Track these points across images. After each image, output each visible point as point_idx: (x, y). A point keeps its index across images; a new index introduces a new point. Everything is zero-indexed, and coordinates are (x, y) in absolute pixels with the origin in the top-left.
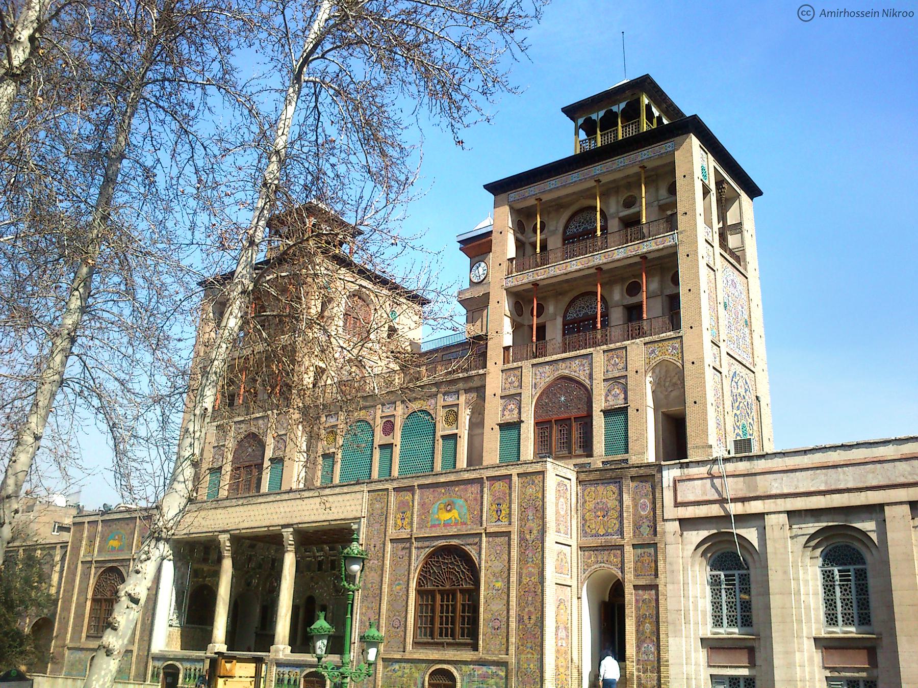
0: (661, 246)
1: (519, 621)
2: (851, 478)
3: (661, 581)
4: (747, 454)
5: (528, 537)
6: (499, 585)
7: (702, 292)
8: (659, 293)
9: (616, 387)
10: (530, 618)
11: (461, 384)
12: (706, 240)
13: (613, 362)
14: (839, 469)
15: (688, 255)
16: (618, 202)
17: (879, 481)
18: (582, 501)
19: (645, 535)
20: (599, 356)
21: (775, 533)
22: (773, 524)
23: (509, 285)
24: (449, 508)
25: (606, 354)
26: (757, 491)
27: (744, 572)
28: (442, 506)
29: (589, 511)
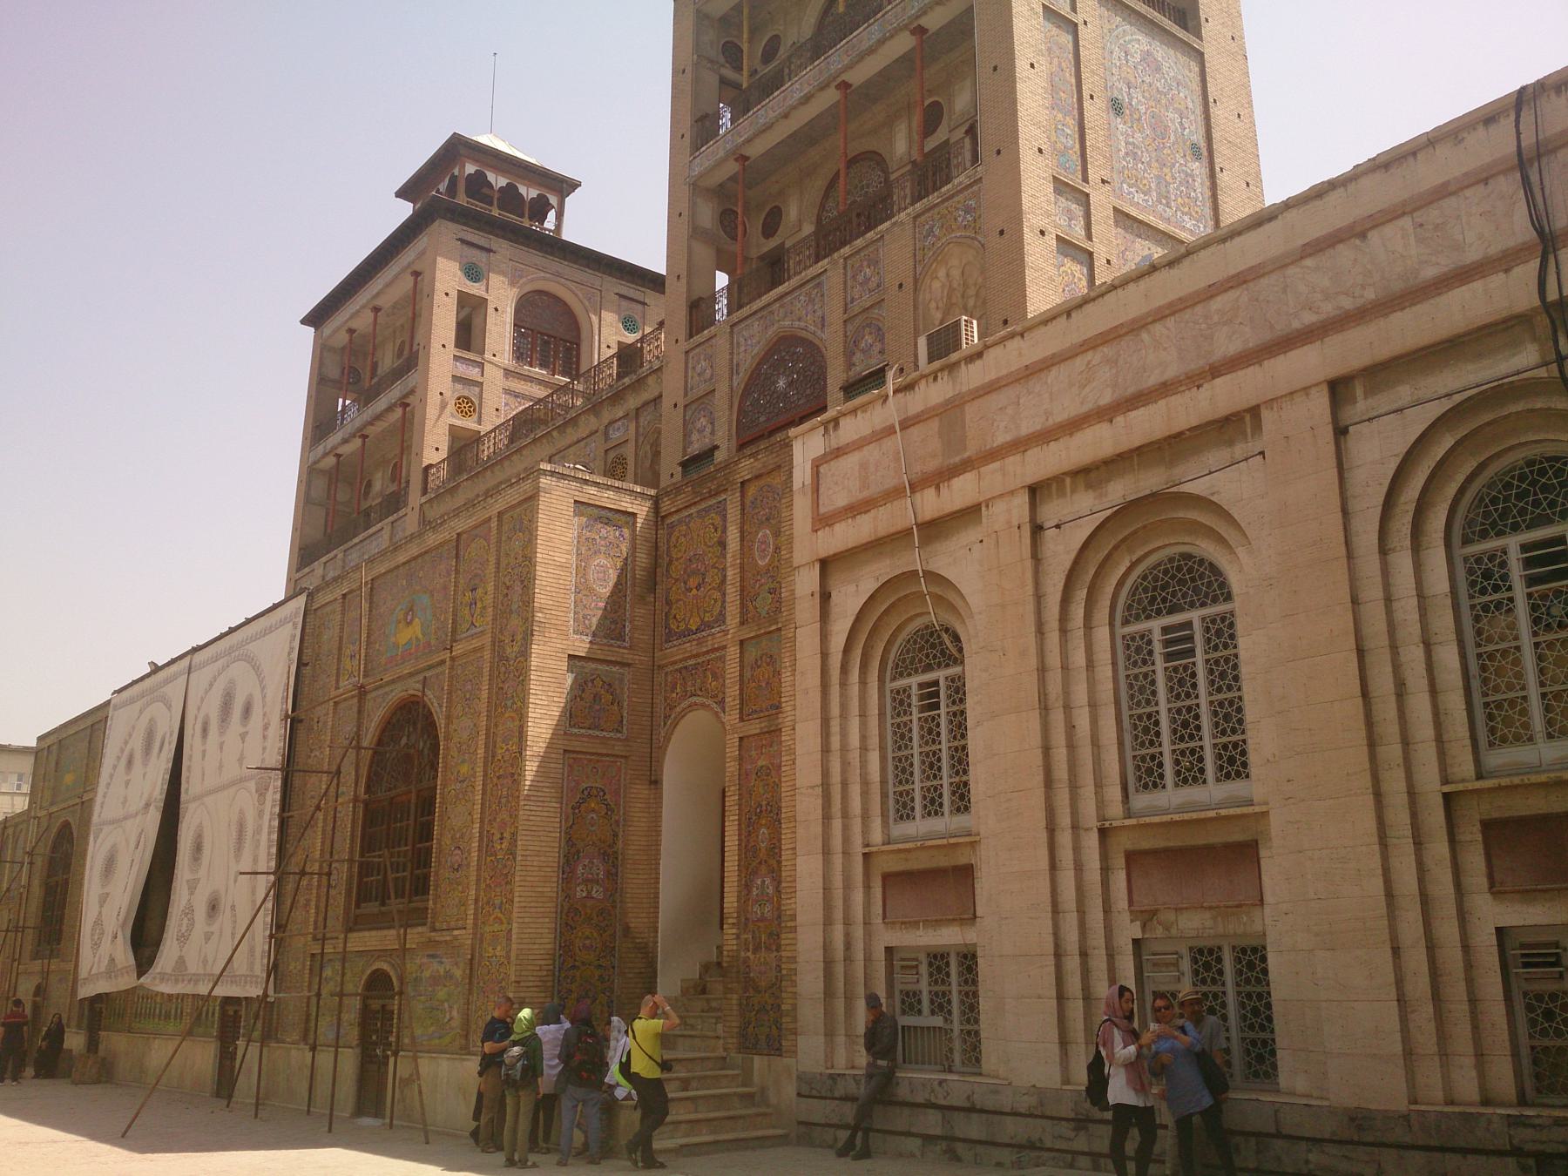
1: (487, 846)
3: (786, 719)
5: (509, 650)
6: (464, 769)
7: (1021, 65)
10: (501, 839)
13: (860, 278)
18: (667, 559)
20: (832, 269)
22: (996, 528)
23: (697, 171)
24: (409, 618)
26: (965, 449)
29: (677, 580)
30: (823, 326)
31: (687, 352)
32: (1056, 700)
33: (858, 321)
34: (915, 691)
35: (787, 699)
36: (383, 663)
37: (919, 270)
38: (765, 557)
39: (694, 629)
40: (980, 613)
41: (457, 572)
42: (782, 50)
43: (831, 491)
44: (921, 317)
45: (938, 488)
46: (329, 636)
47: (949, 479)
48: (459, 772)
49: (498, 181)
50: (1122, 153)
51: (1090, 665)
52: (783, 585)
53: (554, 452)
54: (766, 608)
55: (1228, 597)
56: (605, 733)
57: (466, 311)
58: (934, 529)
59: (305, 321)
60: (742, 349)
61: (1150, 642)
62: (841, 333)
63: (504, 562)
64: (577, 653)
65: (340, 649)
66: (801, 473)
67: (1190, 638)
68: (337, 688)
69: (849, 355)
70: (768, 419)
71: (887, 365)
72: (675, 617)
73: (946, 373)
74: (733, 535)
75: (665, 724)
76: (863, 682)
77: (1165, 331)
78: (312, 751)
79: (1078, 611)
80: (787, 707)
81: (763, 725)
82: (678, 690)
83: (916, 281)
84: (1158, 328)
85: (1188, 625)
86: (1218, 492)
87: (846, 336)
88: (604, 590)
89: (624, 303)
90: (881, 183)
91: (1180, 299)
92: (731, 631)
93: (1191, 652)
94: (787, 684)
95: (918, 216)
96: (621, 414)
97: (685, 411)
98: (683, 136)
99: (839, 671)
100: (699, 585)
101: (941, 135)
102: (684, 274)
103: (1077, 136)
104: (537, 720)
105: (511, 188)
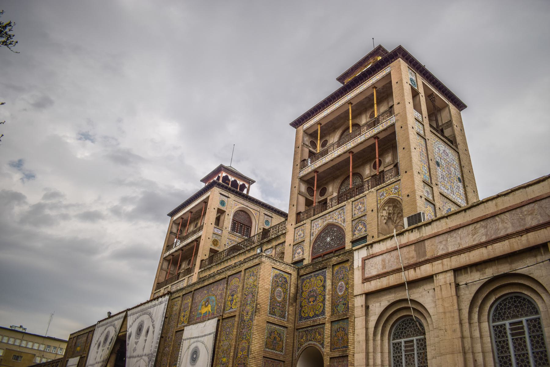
0: (385, 127)
2: (509, 225)
3: (350, 352)
4: (416, 225)
5: (245, 318)
6: (224, 360)
8: (392, 162)
9: (360, 224)
11: (274, 243)
12: (415, 119)
13: (358, 208)
14: (497, 218)
15: (401, 127)
16: (366, 116)
17: (539, 221)
19: (341, 313)
20: (348, 205)
21: (443, 293)
22: (441, 284)
24: (207, 304)
25: (354, 203)
27: (422, 337)
28: (204, 303)
29: (305, 298)
30: (344, 222)
31: (295, 228)
32: (469, 349)
33: (356, 221)
34: (403, 344)
35: (351, 344)
36: (195, 319)
37: (379, 206)
38: (341, 292)
39: (311, 316)
40: (434, 315)
41: (227, 289)
42: (328, 144)
43: (370, 269)
44: (379, 221)
45: (415, 269)
46: (176, 308)
47: (419, 266)
48: (222, 361)
49: (232, 178)
50: (440, 177)
51: (481, 337)
52: (349, 302)
53: (245, 258)
54: (342, 310)
55: (537, 312)
56: (277, 352)
57: (219, 214)
58: (413, 283)
59: (168, 215)
60: (315, 228)
61: (505, 329)
62: (351, 225)
63: (245, 286)
64: (270, 321)
65: (180, 313)
66: (357, 261)
67: (522, 328)
68: (177, 327)
69: (353, 231)
70: (323, 251)
71: (368, 235)
72: (304, 312)
73: (417, 230)
74: (329, 283)
75: (298, 351)
76: (382, 340)
77: (505, 217)
78: (165, 348)
79: (475, 316)
80: (350, 347)
81: (340, 353)
82: (304, 338)
83: (378, 209)
84: (503, 216)
85: (521, 322)
86: (532, 273)
87: (352, 225)
88: (280, 300)
89: (266, 217)
90: (360, 182)
91: (510, 206)
92: (327, 318)
93: (523, 333)
94: (351, 339)
95: (379, 190)
96: (270, 247)
97: (293, 247)
98: (297, 165)
99: (372, 335)
100: (314, 301)
101: (381, 169)
102: (295, 204)
103: (428, 170)
104: (255, 344)
105: (235, 181)
